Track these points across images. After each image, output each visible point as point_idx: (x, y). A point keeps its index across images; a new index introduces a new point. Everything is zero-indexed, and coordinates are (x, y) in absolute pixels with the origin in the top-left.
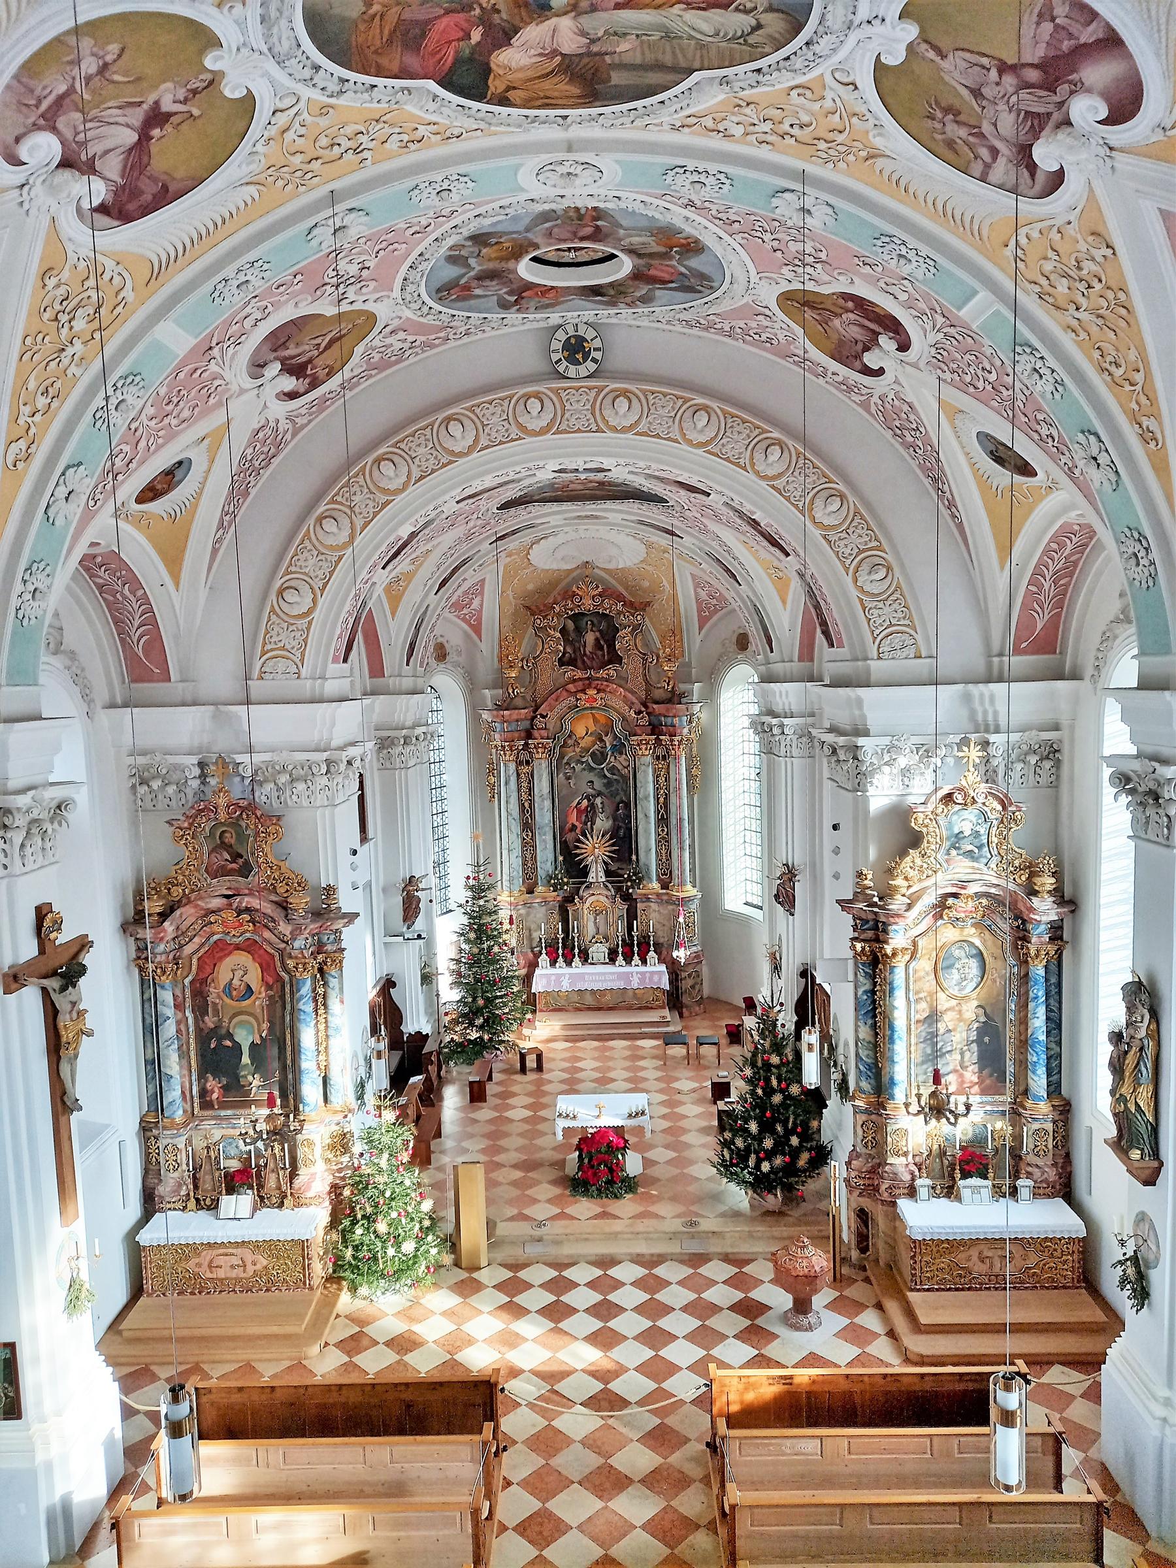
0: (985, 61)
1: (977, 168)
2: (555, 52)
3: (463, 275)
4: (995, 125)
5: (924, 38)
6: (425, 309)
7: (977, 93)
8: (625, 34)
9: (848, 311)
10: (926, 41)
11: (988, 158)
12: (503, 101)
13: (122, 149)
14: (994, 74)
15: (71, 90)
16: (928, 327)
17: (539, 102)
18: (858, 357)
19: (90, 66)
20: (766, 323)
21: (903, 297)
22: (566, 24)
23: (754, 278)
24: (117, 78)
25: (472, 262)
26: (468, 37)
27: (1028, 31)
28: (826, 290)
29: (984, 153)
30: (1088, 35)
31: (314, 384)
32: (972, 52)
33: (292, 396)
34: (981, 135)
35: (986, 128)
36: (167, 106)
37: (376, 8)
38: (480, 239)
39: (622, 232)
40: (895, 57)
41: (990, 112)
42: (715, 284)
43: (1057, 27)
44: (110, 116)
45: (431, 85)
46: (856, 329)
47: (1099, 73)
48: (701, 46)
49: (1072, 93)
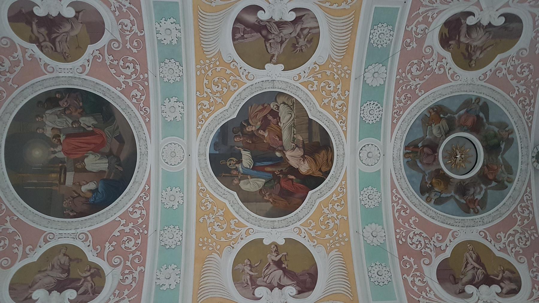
0: (268, 45)
1: (314, 31)
2: (303, 157)
3: (456, 200)
4: (291, 34)
5: (270, 61)
6: (480, 220)
7: (282, 43)
8: (294, 138)
9: (459, 42)
10: (271, 61)
11: (307, 30)
12: (327, 173)
13: (282, 276)
14: (270, 41)
15: (251, 276)
16: (436, 11)
17: (330, 163)
18: (503, 27)
19: (247, 269)
20: (504, 72)
21: (423, 26)
22: (288, 154)
23: (459, 82)
24: (256, 265)
25: (443, 195)
26: (292, 179)
27: (250, 40)
28: (448, 55)
29: (305, 32)
30: (241, 27)
31: (517, 281)
32: (267, 49)
33: (514, 292)
34: (298, 35)
35: (294, 35)
36: (276, 259)
37: (271, 200)
38: (424, 191)
39: (428, 137)
40: (281, 67)
41: (287, 37)
42: (474, 98)
43: (244, 34)
44: (267, 272)
45: (310, 192)
46: (474, 35)
47: (250, 18)
48: (297, 117)
49: (262, 21)
